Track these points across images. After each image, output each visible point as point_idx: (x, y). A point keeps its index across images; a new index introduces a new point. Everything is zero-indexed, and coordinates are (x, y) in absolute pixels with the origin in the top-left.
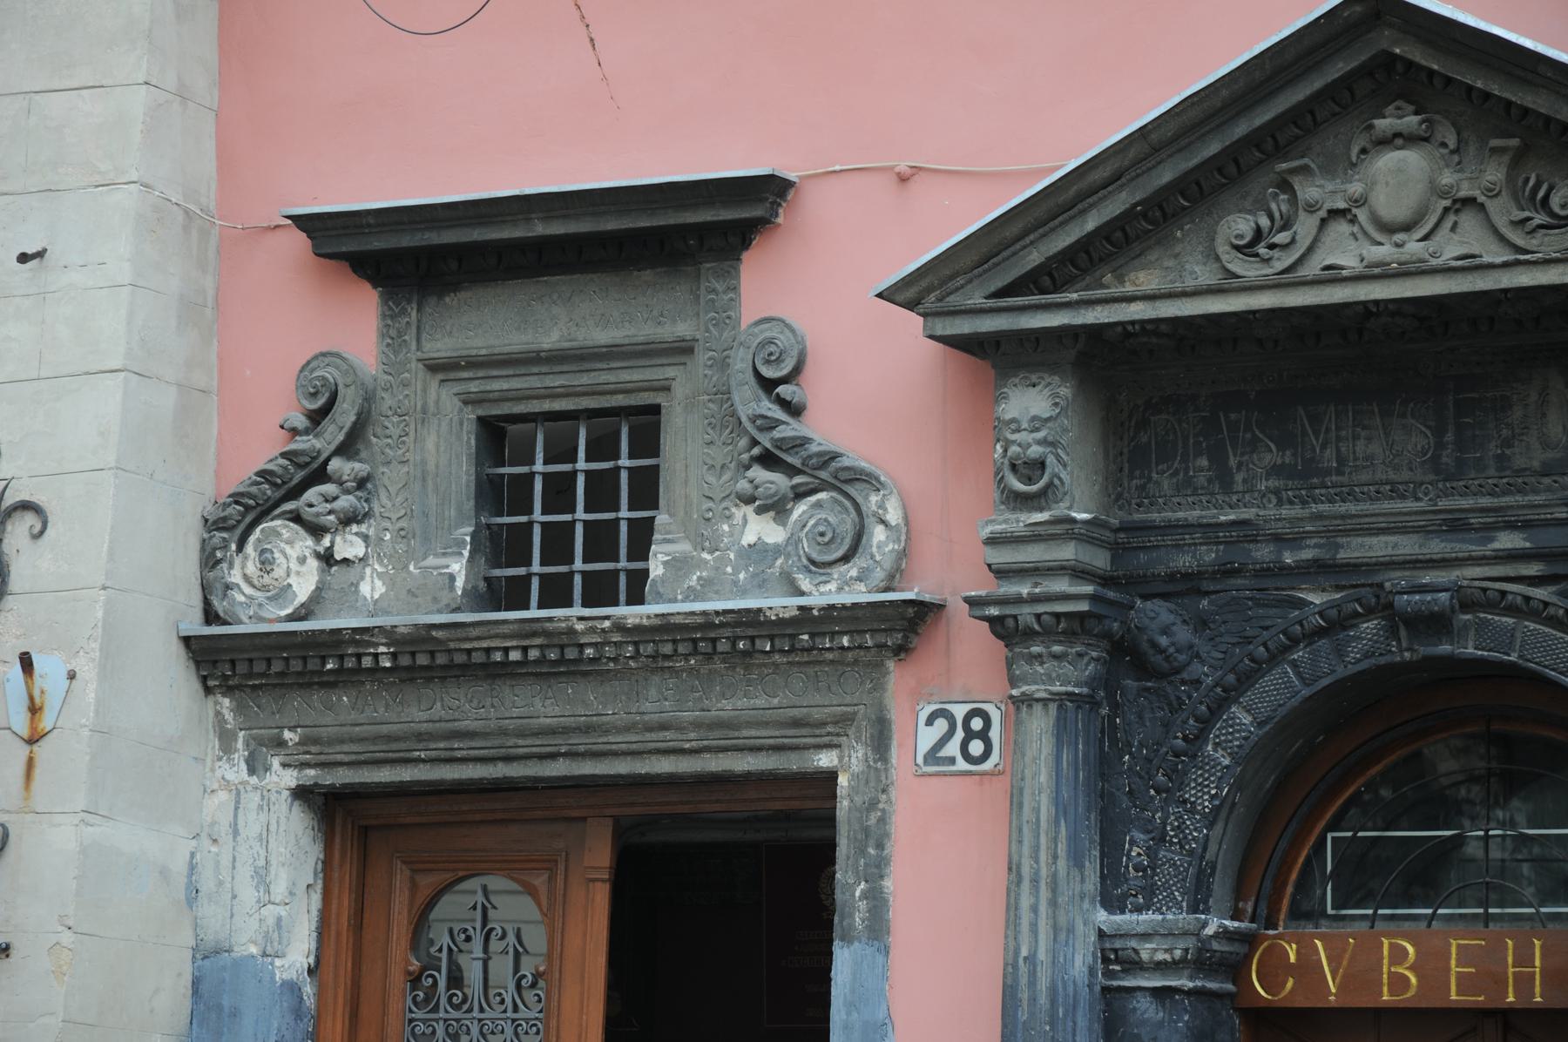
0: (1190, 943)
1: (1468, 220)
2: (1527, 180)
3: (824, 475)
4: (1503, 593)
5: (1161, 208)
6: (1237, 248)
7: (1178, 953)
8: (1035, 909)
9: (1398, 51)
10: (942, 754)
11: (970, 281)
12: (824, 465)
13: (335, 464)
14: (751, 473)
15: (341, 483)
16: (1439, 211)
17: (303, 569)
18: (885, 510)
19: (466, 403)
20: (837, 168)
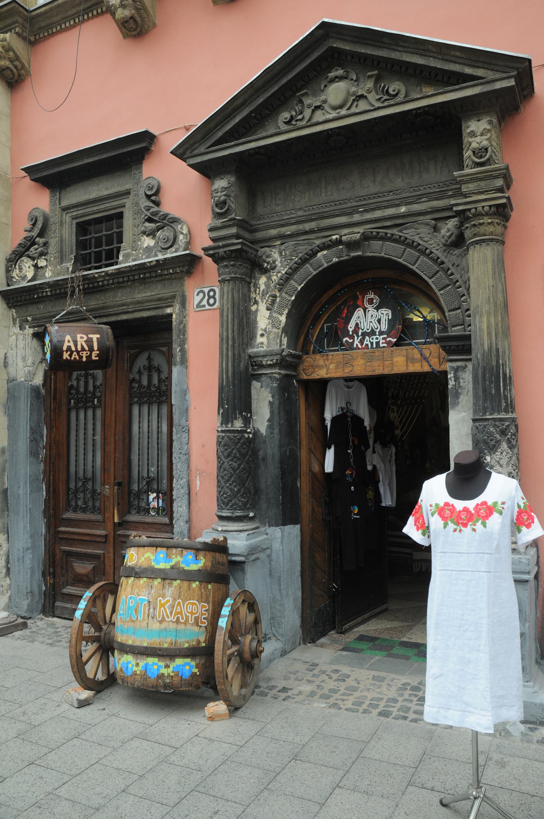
0: (278, 357)
2: (381, 86)
3: (165, 221)
4: (378, 233)
5: (261, 115)
7: (274, 361)
9: (335, 45)
11: (200, 145)
12: (164, 219)
13: (37, 239)
14: (145, 225)
15: (39, 245)
16: (351, 100)
17: (30, 270)
19: (73, 219)
20: (168, 130)
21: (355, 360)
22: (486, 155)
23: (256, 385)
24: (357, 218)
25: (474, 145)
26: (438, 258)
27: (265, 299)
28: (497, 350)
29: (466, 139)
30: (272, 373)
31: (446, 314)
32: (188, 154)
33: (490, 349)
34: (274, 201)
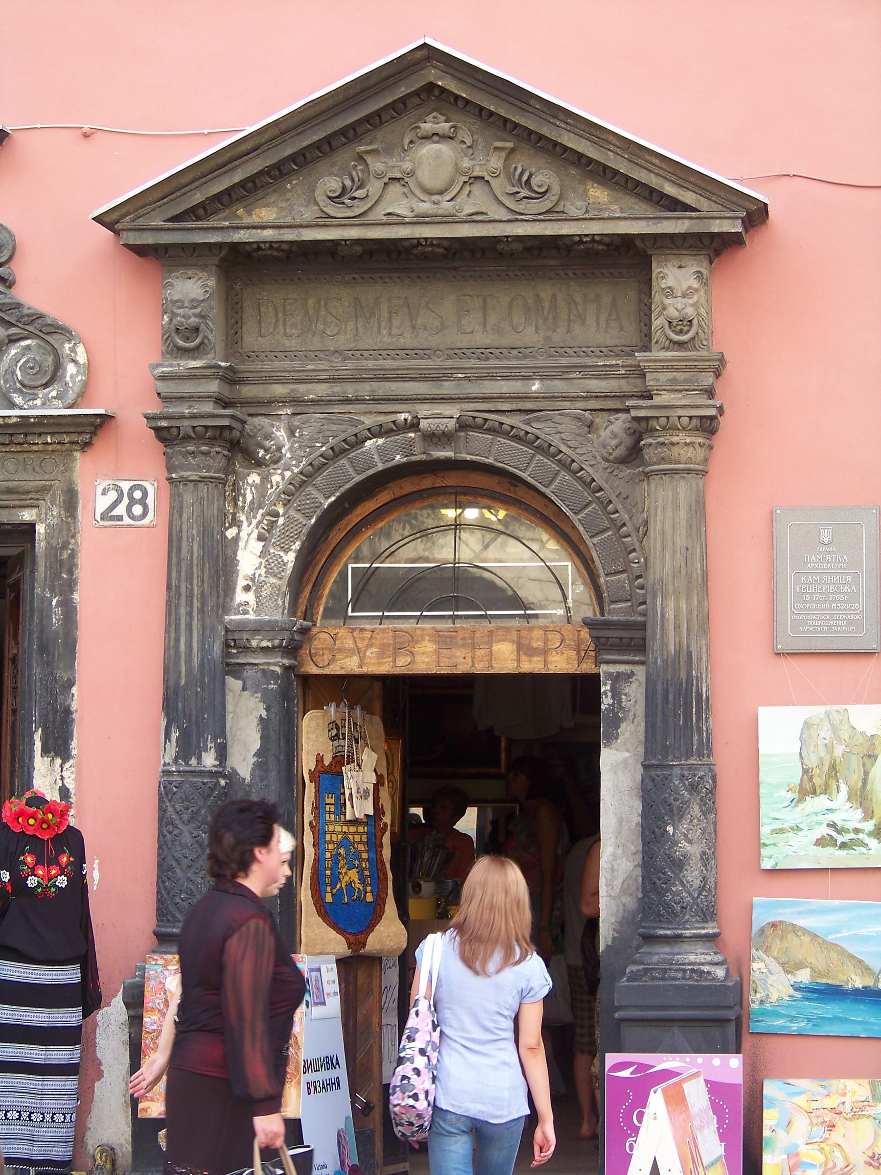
0: (287, 634)
1: (478, 189)
2: (516, 168)
4: (486, 420)
6: (330, 198)
7: (277, 642)
8: (190, 614)
9: (440, 83)
10: (116, 512)
16: (461, 184)
18: (76, 353)
20: (39, 126)
21: (418, 642)
22: (689, 331)
23: (234, 684)
24: (447, 388)
25: (672, 312)
26: (593, 480)
27: (255, 517)
28: (690, 654)
29: (657, 298)
30: (269, 664)
31: (602, 580)
32: (126, 222)
33: (678, 653)
34: (281, 328)
